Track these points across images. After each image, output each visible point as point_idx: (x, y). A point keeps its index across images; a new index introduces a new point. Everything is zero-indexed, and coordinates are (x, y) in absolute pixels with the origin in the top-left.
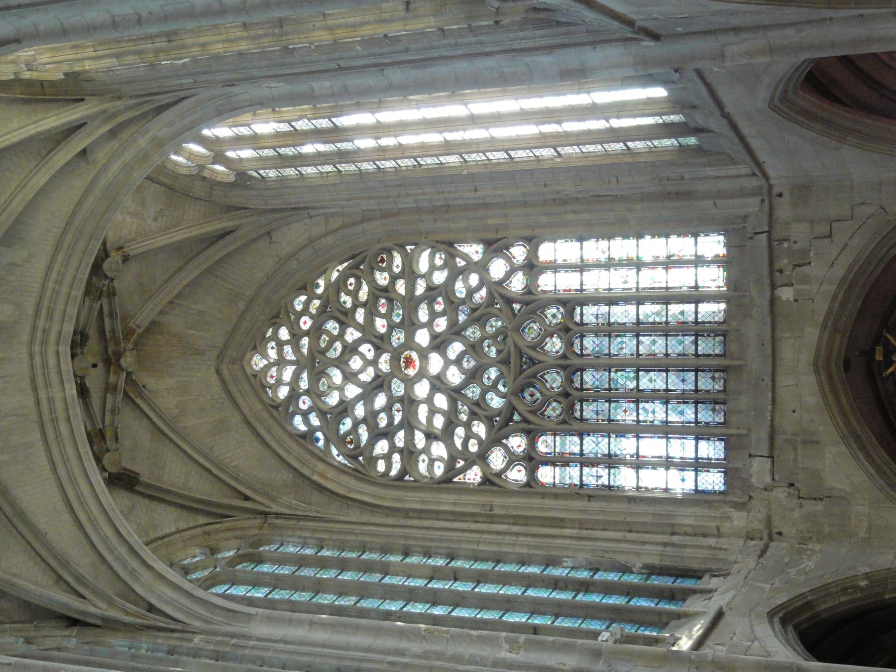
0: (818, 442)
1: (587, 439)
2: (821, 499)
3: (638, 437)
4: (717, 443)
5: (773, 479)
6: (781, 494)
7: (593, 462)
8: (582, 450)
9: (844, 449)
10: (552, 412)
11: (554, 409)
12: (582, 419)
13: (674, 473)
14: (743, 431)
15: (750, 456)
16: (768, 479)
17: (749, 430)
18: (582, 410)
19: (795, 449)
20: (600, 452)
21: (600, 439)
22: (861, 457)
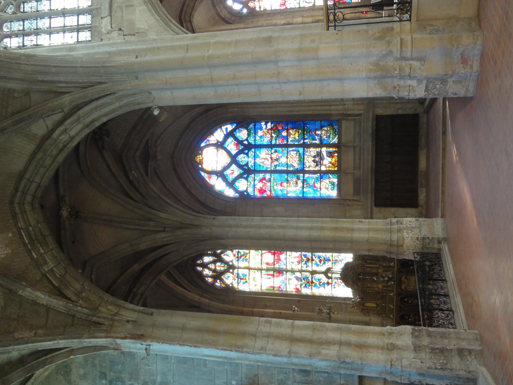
0: (132, 6)
1: (26, 22)
2: (134, 35)
3: (50, 18)
4: (88, 16)
5: (112, 27)
6: (115, 34)
7: (29, 34)
8: (24, 28)
9: (145, 7)
10: (10, 10)
11: (11, 9)
12: (24, 12)
13: (67, 34)
14: (99, 6)
15: (102, 18)
16: (109, 27)
17: (101, 5)
18: (24, 7)
19: (122, 11)
20: (33, 28)
21: (33, 21)
22: (154, 12)
